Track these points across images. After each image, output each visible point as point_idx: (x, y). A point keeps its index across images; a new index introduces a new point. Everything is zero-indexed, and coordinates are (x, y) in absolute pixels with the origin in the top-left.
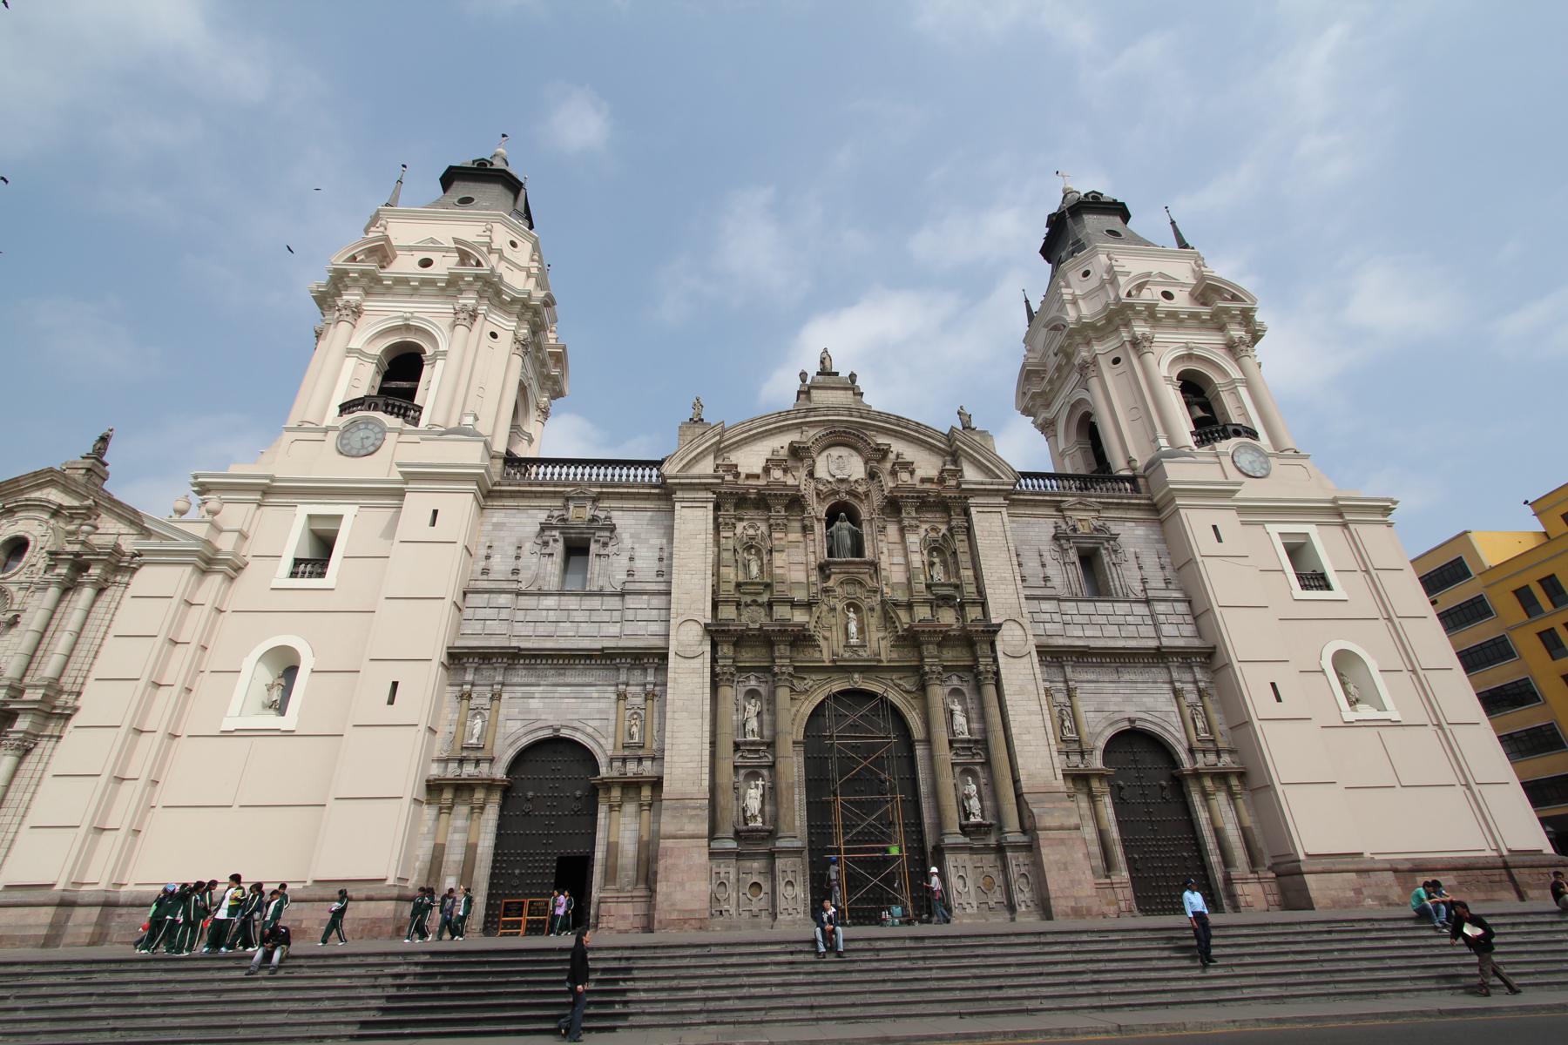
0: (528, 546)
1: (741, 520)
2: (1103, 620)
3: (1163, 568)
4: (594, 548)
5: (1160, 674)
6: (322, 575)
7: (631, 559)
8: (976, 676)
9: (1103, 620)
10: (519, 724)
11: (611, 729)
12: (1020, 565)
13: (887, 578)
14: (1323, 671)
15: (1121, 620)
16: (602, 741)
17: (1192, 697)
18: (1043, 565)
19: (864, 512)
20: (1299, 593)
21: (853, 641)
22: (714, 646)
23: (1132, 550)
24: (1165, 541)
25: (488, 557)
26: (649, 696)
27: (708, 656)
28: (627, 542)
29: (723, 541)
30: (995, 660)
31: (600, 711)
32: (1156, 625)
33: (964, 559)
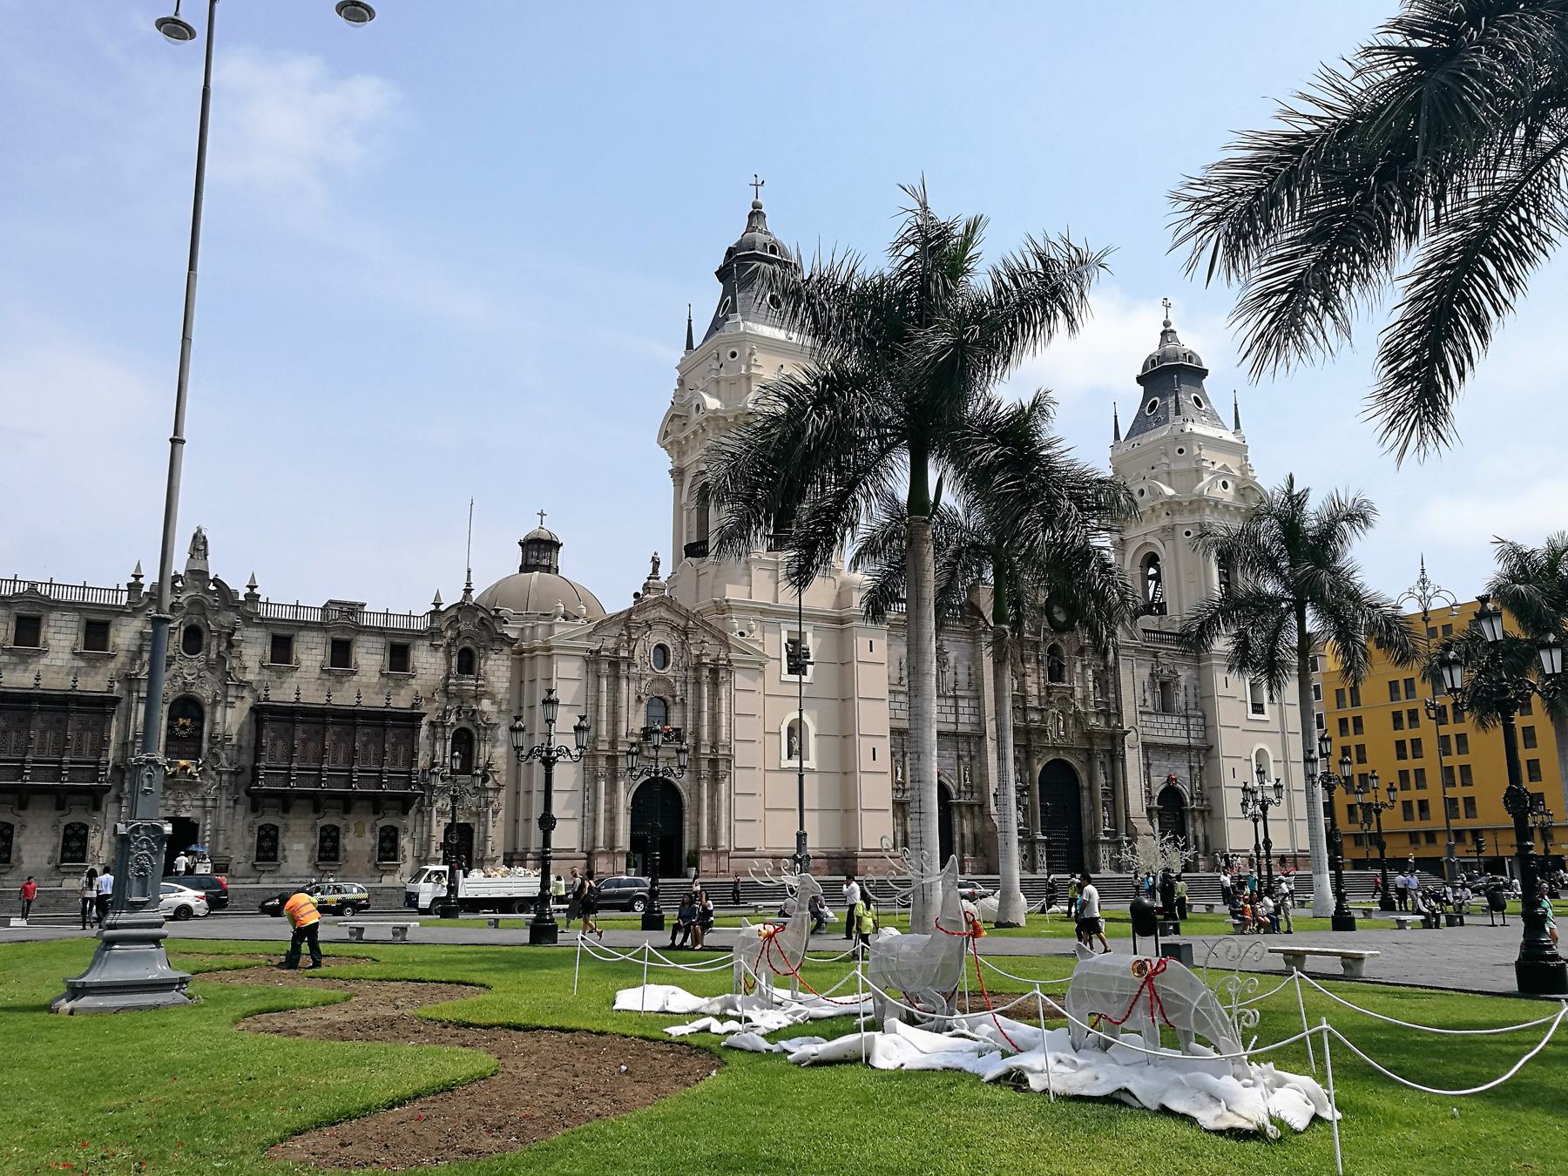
2: (1166, 726)
3: (1196, 696)
5: (1185, 756)
7: (956, 674)
8: (1111, 756)
9: (1166, 726)
14: (1250, 760)
15: (1174, 726)
17: (1197, 770)
19: (1064, 650)
20: (1252, 716)
21: (1062, 733)
24: (1198, 679)
26: (972, 758)
30: (1124, 748)
31: (950, 765)
32: (1188, 731)
33: (1111, 686)
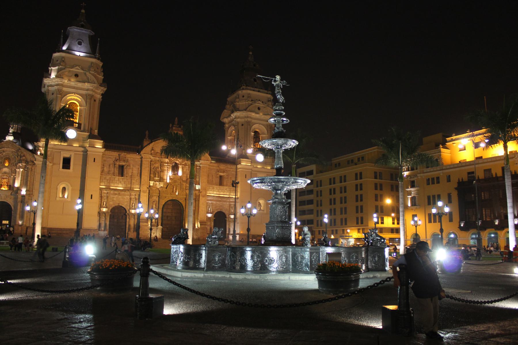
0: (111, 166)
1: (155, 163)
4: (125, 167)
6: (68, 168)
7: (132, 170)
10: (112, 203)
11: (129, 205)
12: (208, 178)
13: (182, 179)
16: (127, 207)
18: (212, 178)
22: (149, 191)
23: (230, 176)
25: (103, 167)
27: (148, 193)
28: (132, 166)
29: (151, 169)
30: (199, 198)
